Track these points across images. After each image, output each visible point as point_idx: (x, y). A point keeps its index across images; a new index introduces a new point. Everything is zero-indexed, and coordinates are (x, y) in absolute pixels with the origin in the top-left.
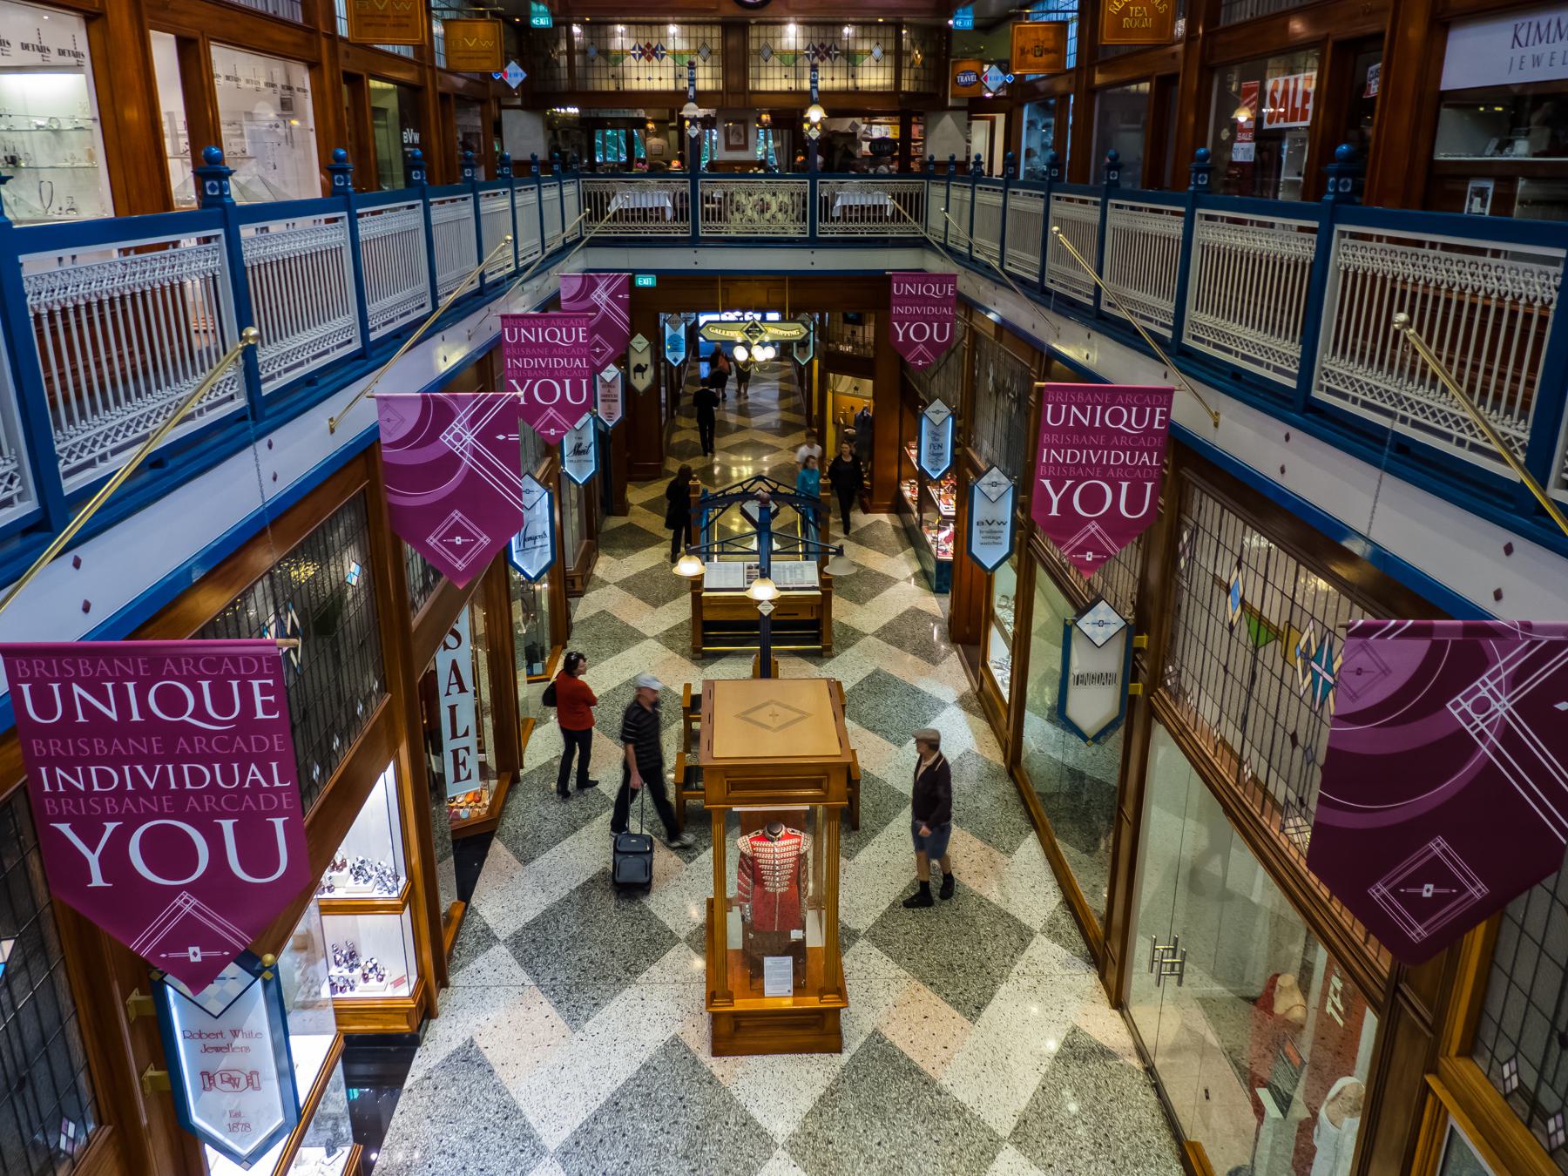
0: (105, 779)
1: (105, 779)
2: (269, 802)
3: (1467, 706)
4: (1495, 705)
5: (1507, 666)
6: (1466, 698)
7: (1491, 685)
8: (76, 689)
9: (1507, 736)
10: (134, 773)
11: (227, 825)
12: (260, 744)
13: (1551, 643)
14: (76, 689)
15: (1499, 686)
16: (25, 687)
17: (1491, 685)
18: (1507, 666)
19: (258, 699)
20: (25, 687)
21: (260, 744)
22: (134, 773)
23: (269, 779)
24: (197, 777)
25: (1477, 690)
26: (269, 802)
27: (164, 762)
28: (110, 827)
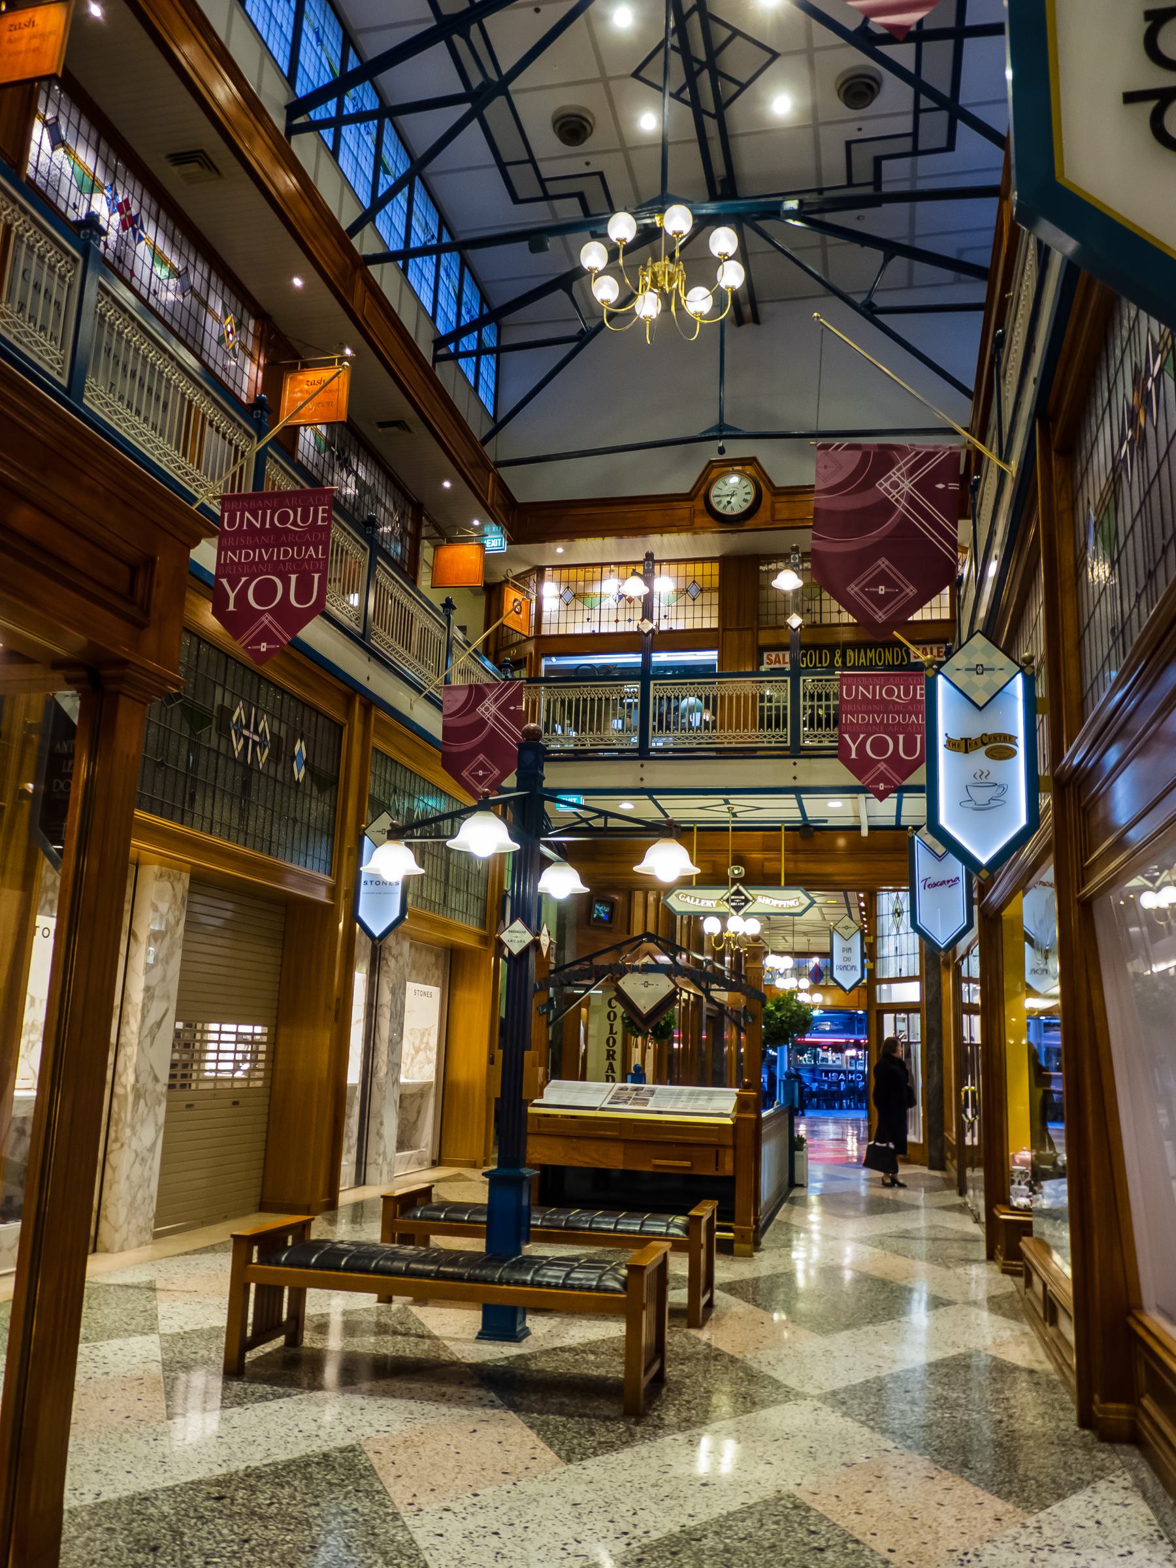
0: (247, 555)
1: (247, 555)
2: (314, 565)
3: (887, 485)
4: (902, 485)
5: (905, 465)
6: (886, 481)
7: (898, 474)
8: (247, 514)
9: (911, 501)
10: (260, 553)
11: (293, 577)
12: (316, 536)
13: (927, 453)
14: (247, 514)
15: (902, 475)
16: (226, 514)
17: (898, 474)
18: (905, 465)
19: (320, 515)
20: (226, 514)
21: (316, 536)
22: (260, 553)
23: (317, 554)
24: (286, 553)
25: (891, 477)
26: (314, 565)
27: (273, 547)
28: (244, 579)
